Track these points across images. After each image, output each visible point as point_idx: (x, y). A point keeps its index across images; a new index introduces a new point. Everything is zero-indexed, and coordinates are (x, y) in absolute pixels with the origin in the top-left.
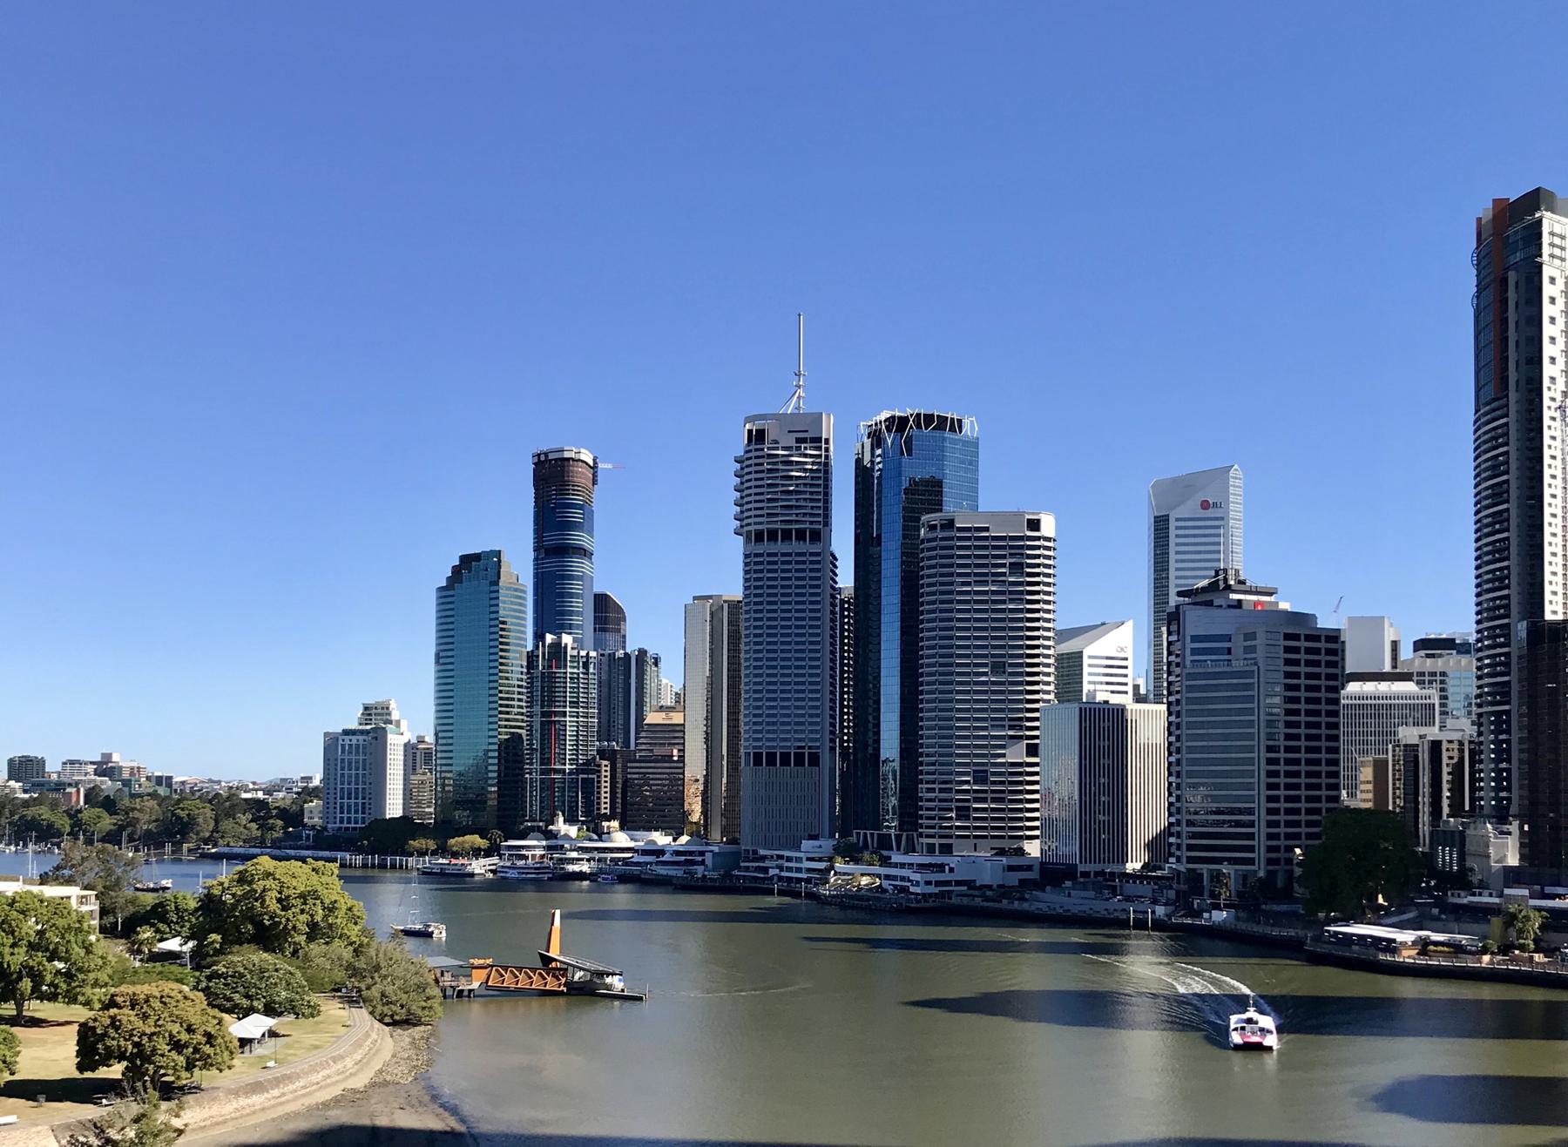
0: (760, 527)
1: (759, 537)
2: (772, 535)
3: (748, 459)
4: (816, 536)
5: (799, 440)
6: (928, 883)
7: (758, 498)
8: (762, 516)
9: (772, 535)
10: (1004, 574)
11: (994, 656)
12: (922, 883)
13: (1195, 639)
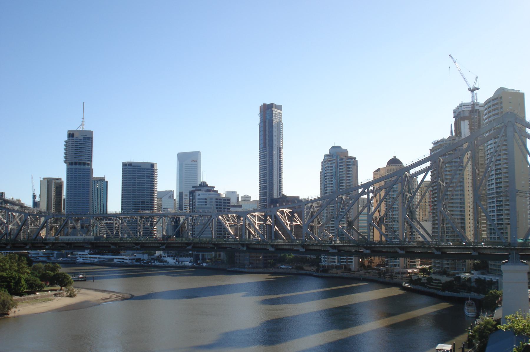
0: (72, 161)
1: (72, 164)
2: (76, 163)
3: (69, 142)
4: (88, 164)
5: (84, 138)
6: (130, 259)
7: (72, 153)
8: (73, 158)
9: (76, 163)
10: (145, 178)
11: (142, 200)
12: (128, 259)
13: (199, 199)
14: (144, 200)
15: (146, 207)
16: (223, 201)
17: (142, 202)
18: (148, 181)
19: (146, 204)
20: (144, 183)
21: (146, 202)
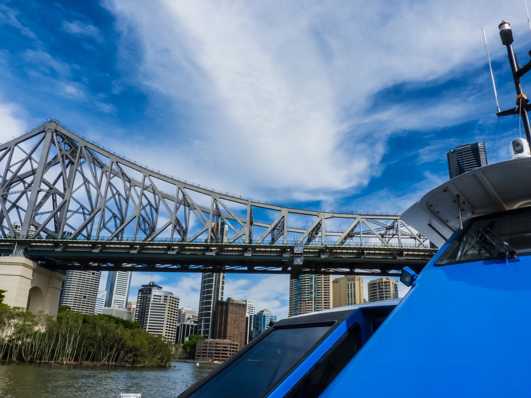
10: (90, 274)
11: (84, 294)
13: (154, 296)
14: (86, 294)
15: (87, 301)
16: (174, 300)
17: (84, 296)
18: (94, 277)
19: (88, 299)
20: (89, 279)
21: (88, 297)
